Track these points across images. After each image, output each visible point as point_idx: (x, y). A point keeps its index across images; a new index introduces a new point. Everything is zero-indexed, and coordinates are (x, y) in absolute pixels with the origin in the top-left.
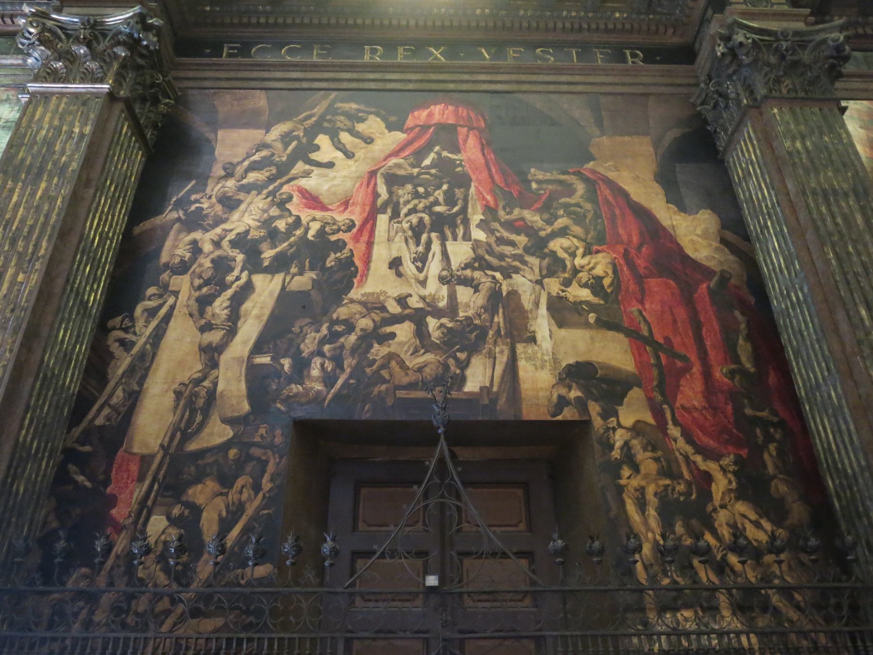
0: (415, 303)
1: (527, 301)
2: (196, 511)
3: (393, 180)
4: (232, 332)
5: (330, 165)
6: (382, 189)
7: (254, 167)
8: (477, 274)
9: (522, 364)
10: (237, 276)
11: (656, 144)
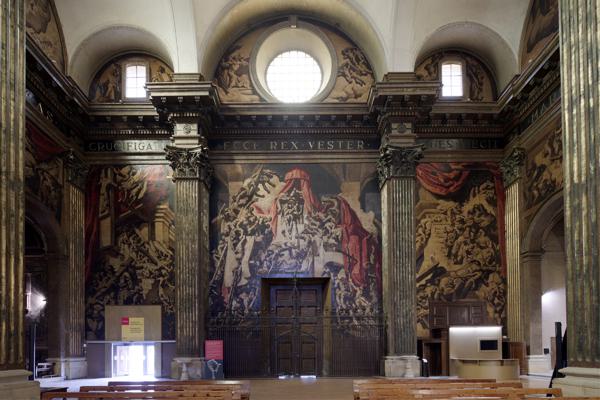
0: (289, 245)
1: (318, 244)
2: (242, 300)
3: (282, 202)
4: (243, 254)
5: (263, 196)
6: (279, 206)
7: (242, 197)
8: (305, 236)
9: (315, 263)
10: (242, 237)
11: (362, 184)
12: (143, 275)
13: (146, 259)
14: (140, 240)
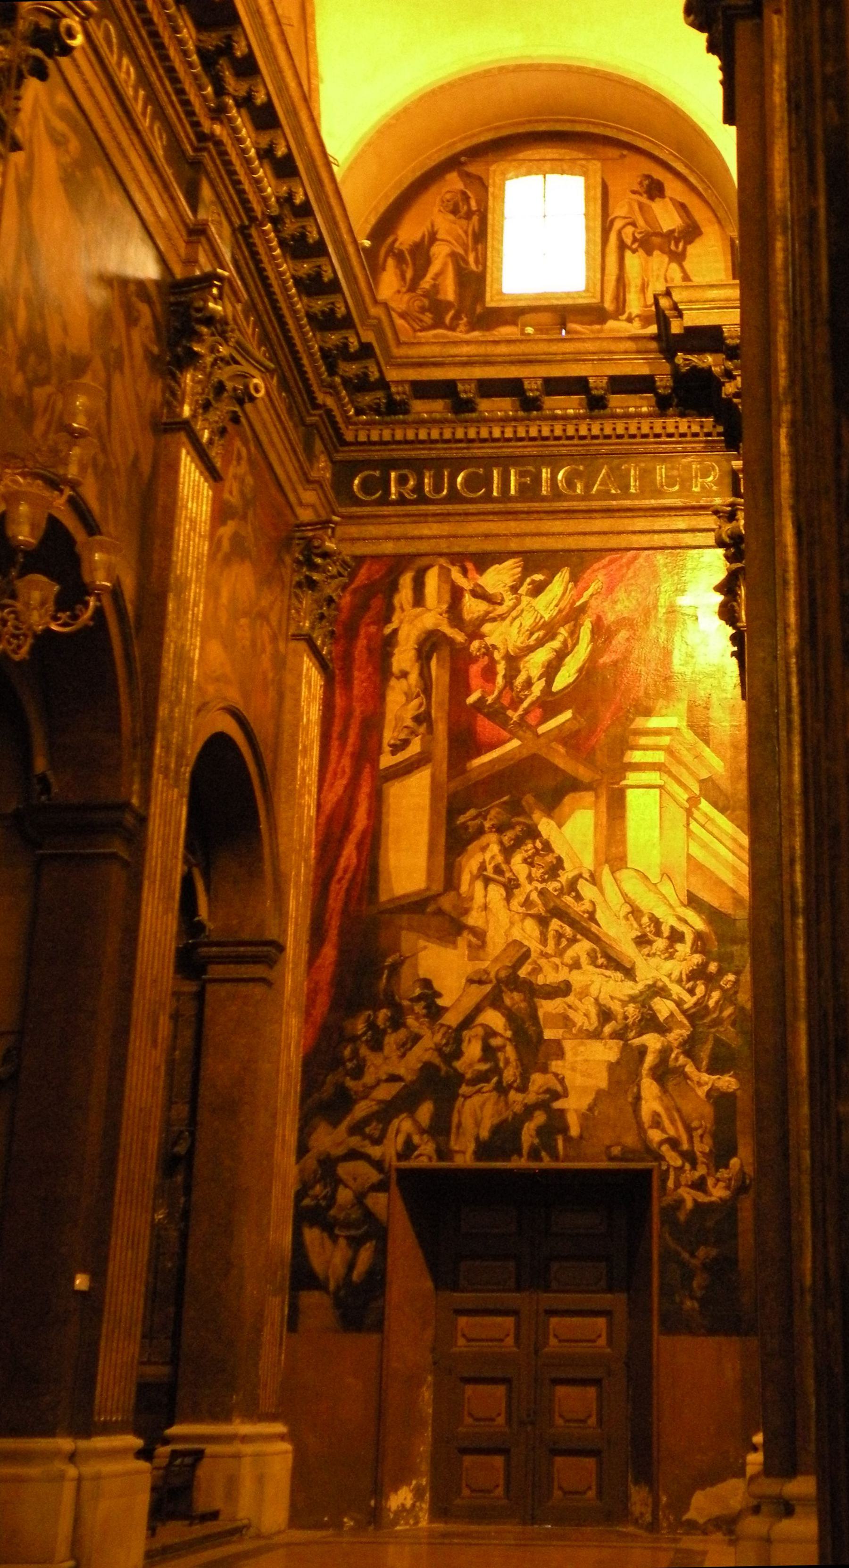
12: (566, 1021)
13: (583, 947)
14: (557, 867)
